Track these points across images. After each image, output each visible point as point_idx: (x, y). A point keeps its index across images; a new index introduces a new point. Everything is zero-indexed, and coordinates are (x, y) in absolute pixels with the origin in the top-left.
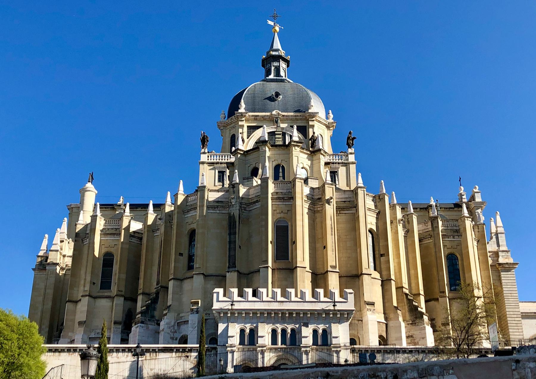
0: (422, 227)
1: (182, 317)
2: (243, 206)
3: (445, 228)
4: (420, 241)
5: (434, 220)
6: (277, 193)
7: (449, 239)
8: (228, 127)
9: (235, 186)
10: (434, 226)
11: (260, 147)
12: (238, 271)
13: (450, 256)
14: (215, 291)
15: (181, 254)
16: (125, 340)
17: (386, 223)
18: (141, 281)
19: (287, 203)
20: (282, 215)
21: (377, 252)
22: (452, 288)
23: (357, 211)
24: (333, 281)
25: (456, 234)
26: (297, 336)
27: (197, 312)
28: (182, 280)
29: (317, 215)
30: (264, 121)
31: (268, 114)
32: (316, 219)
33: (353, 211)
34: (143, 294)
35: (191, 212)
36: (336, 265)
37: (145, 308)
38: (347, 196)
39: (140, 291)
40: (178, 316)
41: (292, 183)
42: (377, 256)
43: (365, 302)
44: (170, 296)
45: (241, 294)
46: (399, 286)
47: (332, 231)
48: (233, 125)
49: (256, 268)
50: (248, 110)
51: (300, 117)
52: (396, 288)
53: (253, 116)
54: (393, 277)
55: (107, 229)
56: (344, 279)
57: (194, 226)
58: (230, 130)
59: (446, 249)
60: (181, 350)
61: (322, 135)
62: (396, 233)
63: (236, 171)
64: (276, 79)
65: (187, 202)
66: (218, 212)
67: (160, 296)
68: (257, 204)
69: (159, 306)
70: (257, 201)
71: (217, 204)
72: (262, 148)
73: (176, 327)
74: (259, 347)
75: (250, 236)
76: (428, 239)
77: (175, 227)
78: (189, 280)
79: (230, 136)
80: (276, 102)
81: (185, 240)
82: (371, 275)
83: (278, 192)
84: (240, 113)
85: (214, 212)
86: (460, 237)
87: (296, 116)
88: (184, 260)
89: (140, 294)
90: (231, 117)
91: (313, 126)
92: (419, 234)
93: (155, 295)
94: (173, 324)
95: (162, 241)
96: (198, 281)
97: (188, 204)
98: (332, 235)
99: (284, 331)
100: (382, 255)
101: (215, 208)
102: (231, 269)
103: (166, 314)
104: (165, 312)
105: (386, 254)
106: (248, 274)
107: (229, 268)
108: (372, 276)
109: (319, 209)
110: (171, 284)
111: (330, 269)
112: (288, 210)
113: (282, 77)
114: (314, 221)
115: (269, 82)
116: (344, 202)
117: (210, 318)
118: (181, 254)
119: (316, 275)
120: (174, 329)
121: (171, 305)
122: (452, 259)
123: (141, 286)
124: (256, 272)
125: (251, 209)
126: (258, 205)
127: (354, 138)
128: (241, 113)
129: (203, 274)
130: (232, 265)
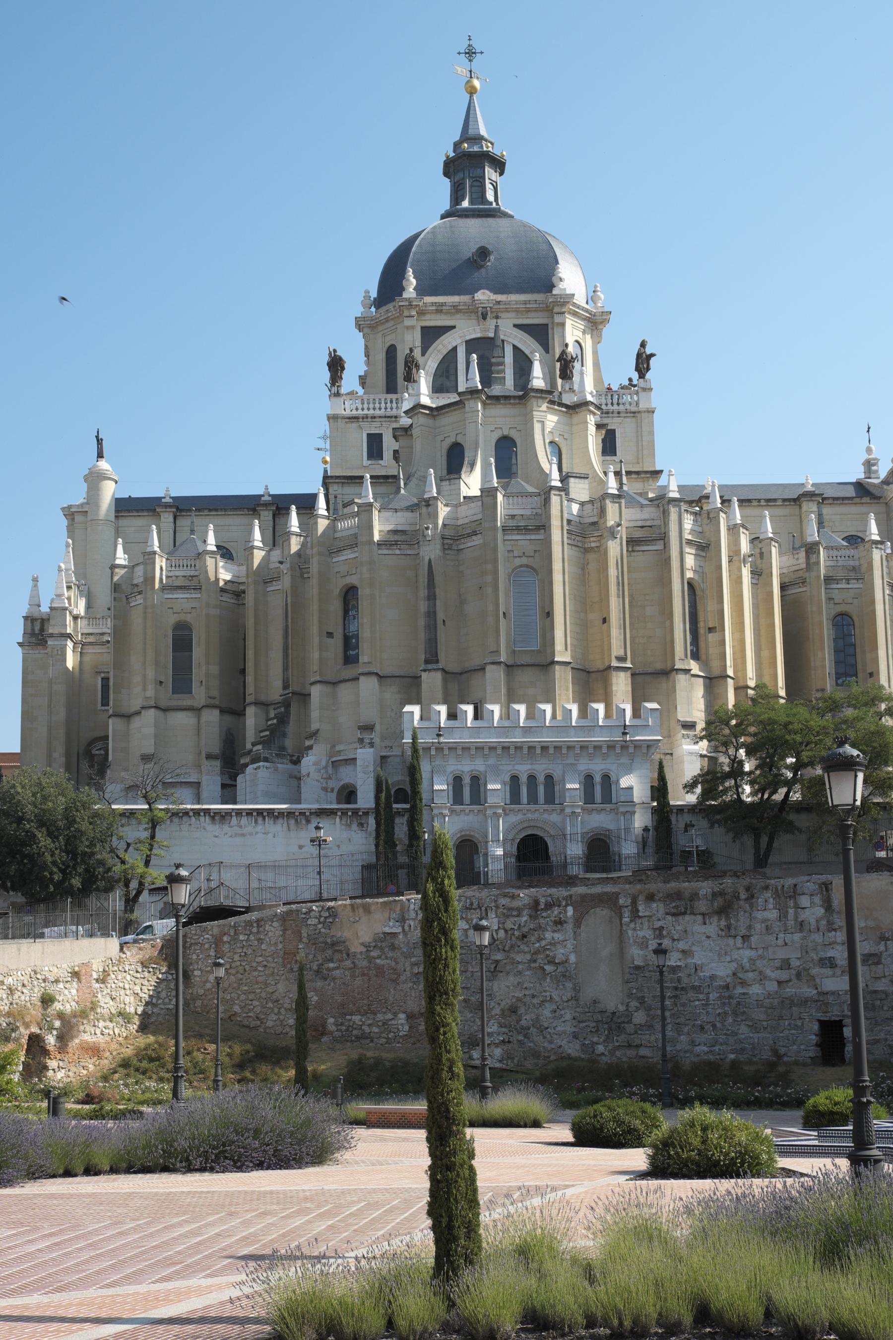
0: (789, 560)
1: (340, 751)
2: (446, 541)
3: (832, 564)
4: (783, 587)
5: (811, 548)
6: (513, 517)
7: (839, 586)
8: (380, 328)
9: (431, 502)
10: (812, 561)
11: (466, 403)
12: (443, 670)
13: (839, 618)
14: (404, 710)
15: (330, 635)
16: (229, 792)
17: (720, 567)
18: (250, 679)
19: (533, 537)
20: (524, 561)
21: (701, 625)
22: (840, 681)
23: (666, 546)
24: (621, 684)
25: (852, 574)
26: (557, 788)
27: (372, 745)
28: (334, 684)
29: (591, 556)
30: (458, 316)
31: (465, 298)
32: (588, 564)
33: (659, 546)
34: (257, 703)
35: (345, 552)
36: (626, 654)
37: (267, 733)
38: (646, 516)
39: (249, 699)
40: (333, 752)
41: (543, 497)
42: (702, 631)
43: (679, 721)
44: (315, 713)
45: (452, 715)
46: (741, 684)
47: (618, 590)
48: (391, 323)
49: (476, 662)
50: (421, 290)
51: (535, 306)
52: (736, 689)
53: (433, 304)
54: (730, 672)
55: (174, 578)
56: (639, 679)
57: (353, 580)
58: (384, 336)
59: (832, 606)
60: (350, 813)
61: (581, 341)
62: (737, 581)
63: (432, 471)
64: (479, 210)
65: (335, 531)
66: (398, 552)
67: (293, 709)
68: (474, 538)
69: (291, 728)
70: (475, 533)
71: (397, 538)
72: (469, 405)
73: (330, 770)
74: (490, 807)
75: (462, 602)
76: (797, 586)
77: (314, 581)
78: (348, 684)
79: (385, 349)
80: (483, 271)
81: (336, 606)
82: (690, 670)
83: (515, 515)
84: (406, 299)
85: (390, 552)
86: (860, 581)
87: (525, 303)
88: (337, 643)
89: (250, 704)
90: (385, 305)
91: (563, 325)
92: (782, 575)
93: (283, 709)
94: (324, 763)
95: (287, 605)
96: (368, 687)
97: (337, 535)
98: (618, 597)
99: (532, 778)
100: (711, 630)
101: (391, 545)
102: (430, 666)
103: (310, 748)
104: (308, 743)
105: (717, 629)
106: (461, 673)
107: (427, 662)
108: (692, 672)
109: (593, 545)
110: (316, 692)
111: (615, 663)
112: (535, 551)
113: (491, 203)
114: (583, 569)
115: (467, 216)
116: (642, 527)
117: (394, 753)
118: (330, 635)
119: (589, 672)
120: (327, 772)
121: (318, 730)
122: (843, 625)
123: (250, 689)
124: (475, 670)
125: (462, 547)
126: (477, 541)
127: (652, 355)
128: (409, 300)
129: (377, 674)
130: (432, 659)
